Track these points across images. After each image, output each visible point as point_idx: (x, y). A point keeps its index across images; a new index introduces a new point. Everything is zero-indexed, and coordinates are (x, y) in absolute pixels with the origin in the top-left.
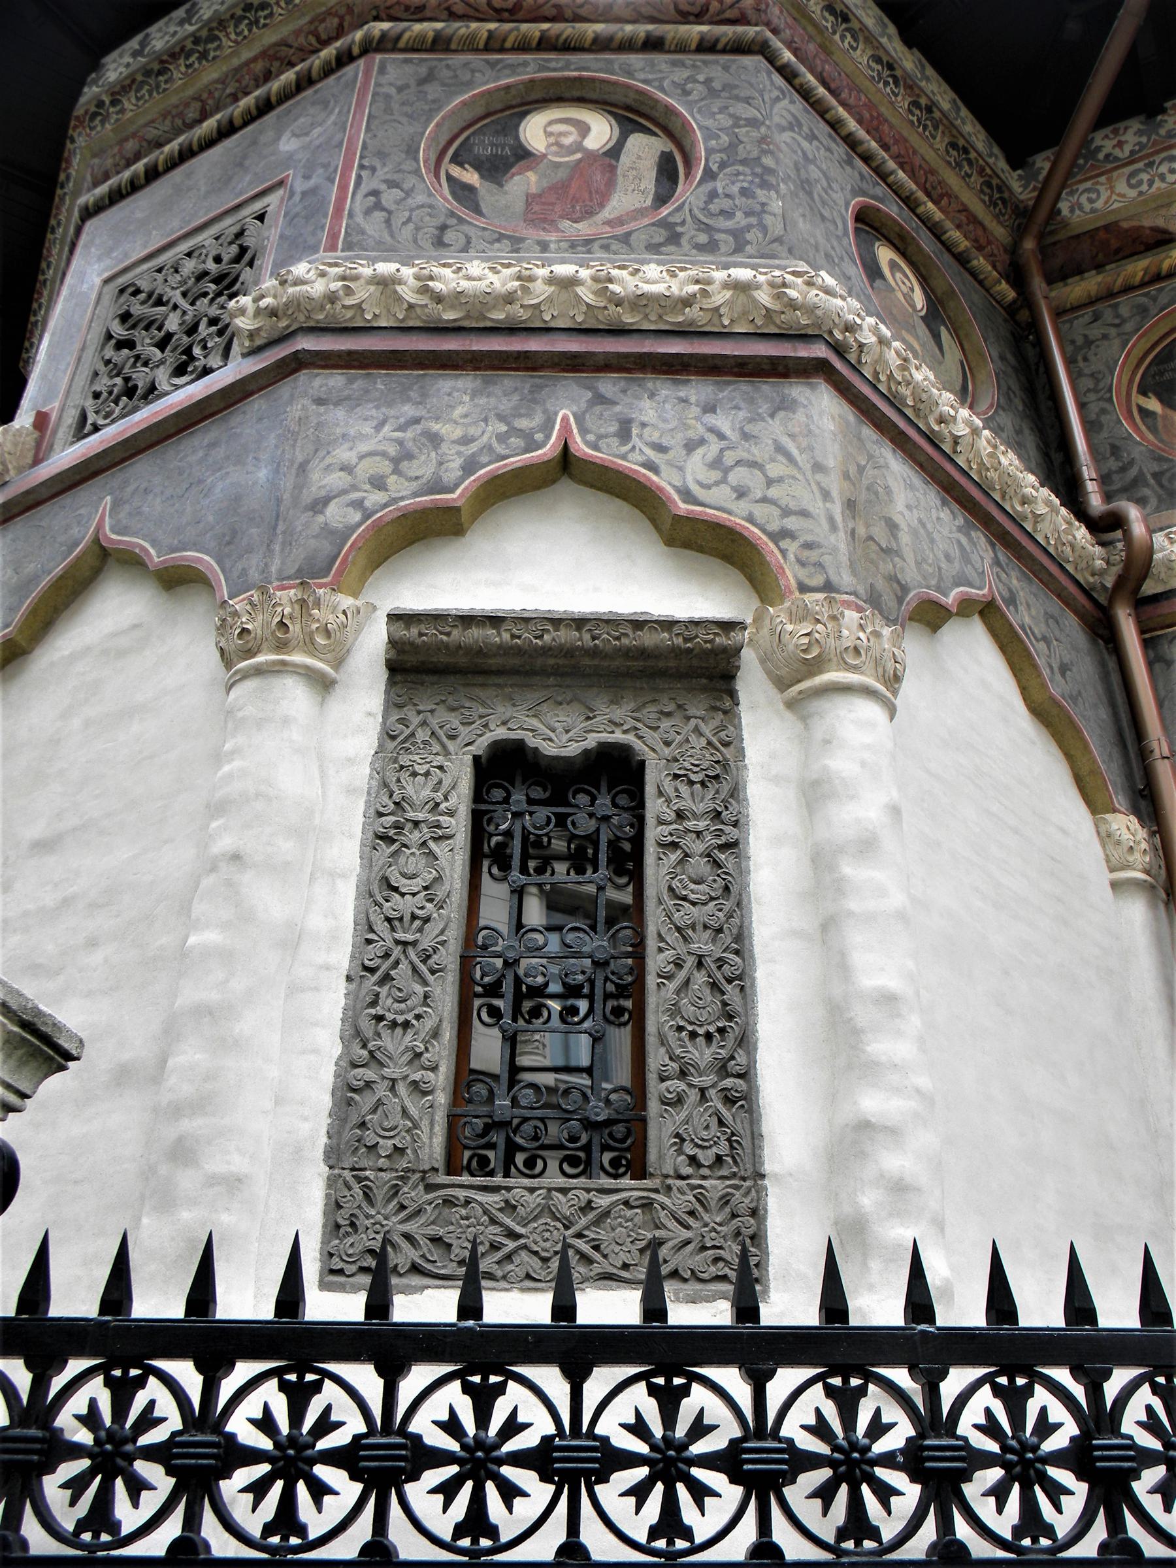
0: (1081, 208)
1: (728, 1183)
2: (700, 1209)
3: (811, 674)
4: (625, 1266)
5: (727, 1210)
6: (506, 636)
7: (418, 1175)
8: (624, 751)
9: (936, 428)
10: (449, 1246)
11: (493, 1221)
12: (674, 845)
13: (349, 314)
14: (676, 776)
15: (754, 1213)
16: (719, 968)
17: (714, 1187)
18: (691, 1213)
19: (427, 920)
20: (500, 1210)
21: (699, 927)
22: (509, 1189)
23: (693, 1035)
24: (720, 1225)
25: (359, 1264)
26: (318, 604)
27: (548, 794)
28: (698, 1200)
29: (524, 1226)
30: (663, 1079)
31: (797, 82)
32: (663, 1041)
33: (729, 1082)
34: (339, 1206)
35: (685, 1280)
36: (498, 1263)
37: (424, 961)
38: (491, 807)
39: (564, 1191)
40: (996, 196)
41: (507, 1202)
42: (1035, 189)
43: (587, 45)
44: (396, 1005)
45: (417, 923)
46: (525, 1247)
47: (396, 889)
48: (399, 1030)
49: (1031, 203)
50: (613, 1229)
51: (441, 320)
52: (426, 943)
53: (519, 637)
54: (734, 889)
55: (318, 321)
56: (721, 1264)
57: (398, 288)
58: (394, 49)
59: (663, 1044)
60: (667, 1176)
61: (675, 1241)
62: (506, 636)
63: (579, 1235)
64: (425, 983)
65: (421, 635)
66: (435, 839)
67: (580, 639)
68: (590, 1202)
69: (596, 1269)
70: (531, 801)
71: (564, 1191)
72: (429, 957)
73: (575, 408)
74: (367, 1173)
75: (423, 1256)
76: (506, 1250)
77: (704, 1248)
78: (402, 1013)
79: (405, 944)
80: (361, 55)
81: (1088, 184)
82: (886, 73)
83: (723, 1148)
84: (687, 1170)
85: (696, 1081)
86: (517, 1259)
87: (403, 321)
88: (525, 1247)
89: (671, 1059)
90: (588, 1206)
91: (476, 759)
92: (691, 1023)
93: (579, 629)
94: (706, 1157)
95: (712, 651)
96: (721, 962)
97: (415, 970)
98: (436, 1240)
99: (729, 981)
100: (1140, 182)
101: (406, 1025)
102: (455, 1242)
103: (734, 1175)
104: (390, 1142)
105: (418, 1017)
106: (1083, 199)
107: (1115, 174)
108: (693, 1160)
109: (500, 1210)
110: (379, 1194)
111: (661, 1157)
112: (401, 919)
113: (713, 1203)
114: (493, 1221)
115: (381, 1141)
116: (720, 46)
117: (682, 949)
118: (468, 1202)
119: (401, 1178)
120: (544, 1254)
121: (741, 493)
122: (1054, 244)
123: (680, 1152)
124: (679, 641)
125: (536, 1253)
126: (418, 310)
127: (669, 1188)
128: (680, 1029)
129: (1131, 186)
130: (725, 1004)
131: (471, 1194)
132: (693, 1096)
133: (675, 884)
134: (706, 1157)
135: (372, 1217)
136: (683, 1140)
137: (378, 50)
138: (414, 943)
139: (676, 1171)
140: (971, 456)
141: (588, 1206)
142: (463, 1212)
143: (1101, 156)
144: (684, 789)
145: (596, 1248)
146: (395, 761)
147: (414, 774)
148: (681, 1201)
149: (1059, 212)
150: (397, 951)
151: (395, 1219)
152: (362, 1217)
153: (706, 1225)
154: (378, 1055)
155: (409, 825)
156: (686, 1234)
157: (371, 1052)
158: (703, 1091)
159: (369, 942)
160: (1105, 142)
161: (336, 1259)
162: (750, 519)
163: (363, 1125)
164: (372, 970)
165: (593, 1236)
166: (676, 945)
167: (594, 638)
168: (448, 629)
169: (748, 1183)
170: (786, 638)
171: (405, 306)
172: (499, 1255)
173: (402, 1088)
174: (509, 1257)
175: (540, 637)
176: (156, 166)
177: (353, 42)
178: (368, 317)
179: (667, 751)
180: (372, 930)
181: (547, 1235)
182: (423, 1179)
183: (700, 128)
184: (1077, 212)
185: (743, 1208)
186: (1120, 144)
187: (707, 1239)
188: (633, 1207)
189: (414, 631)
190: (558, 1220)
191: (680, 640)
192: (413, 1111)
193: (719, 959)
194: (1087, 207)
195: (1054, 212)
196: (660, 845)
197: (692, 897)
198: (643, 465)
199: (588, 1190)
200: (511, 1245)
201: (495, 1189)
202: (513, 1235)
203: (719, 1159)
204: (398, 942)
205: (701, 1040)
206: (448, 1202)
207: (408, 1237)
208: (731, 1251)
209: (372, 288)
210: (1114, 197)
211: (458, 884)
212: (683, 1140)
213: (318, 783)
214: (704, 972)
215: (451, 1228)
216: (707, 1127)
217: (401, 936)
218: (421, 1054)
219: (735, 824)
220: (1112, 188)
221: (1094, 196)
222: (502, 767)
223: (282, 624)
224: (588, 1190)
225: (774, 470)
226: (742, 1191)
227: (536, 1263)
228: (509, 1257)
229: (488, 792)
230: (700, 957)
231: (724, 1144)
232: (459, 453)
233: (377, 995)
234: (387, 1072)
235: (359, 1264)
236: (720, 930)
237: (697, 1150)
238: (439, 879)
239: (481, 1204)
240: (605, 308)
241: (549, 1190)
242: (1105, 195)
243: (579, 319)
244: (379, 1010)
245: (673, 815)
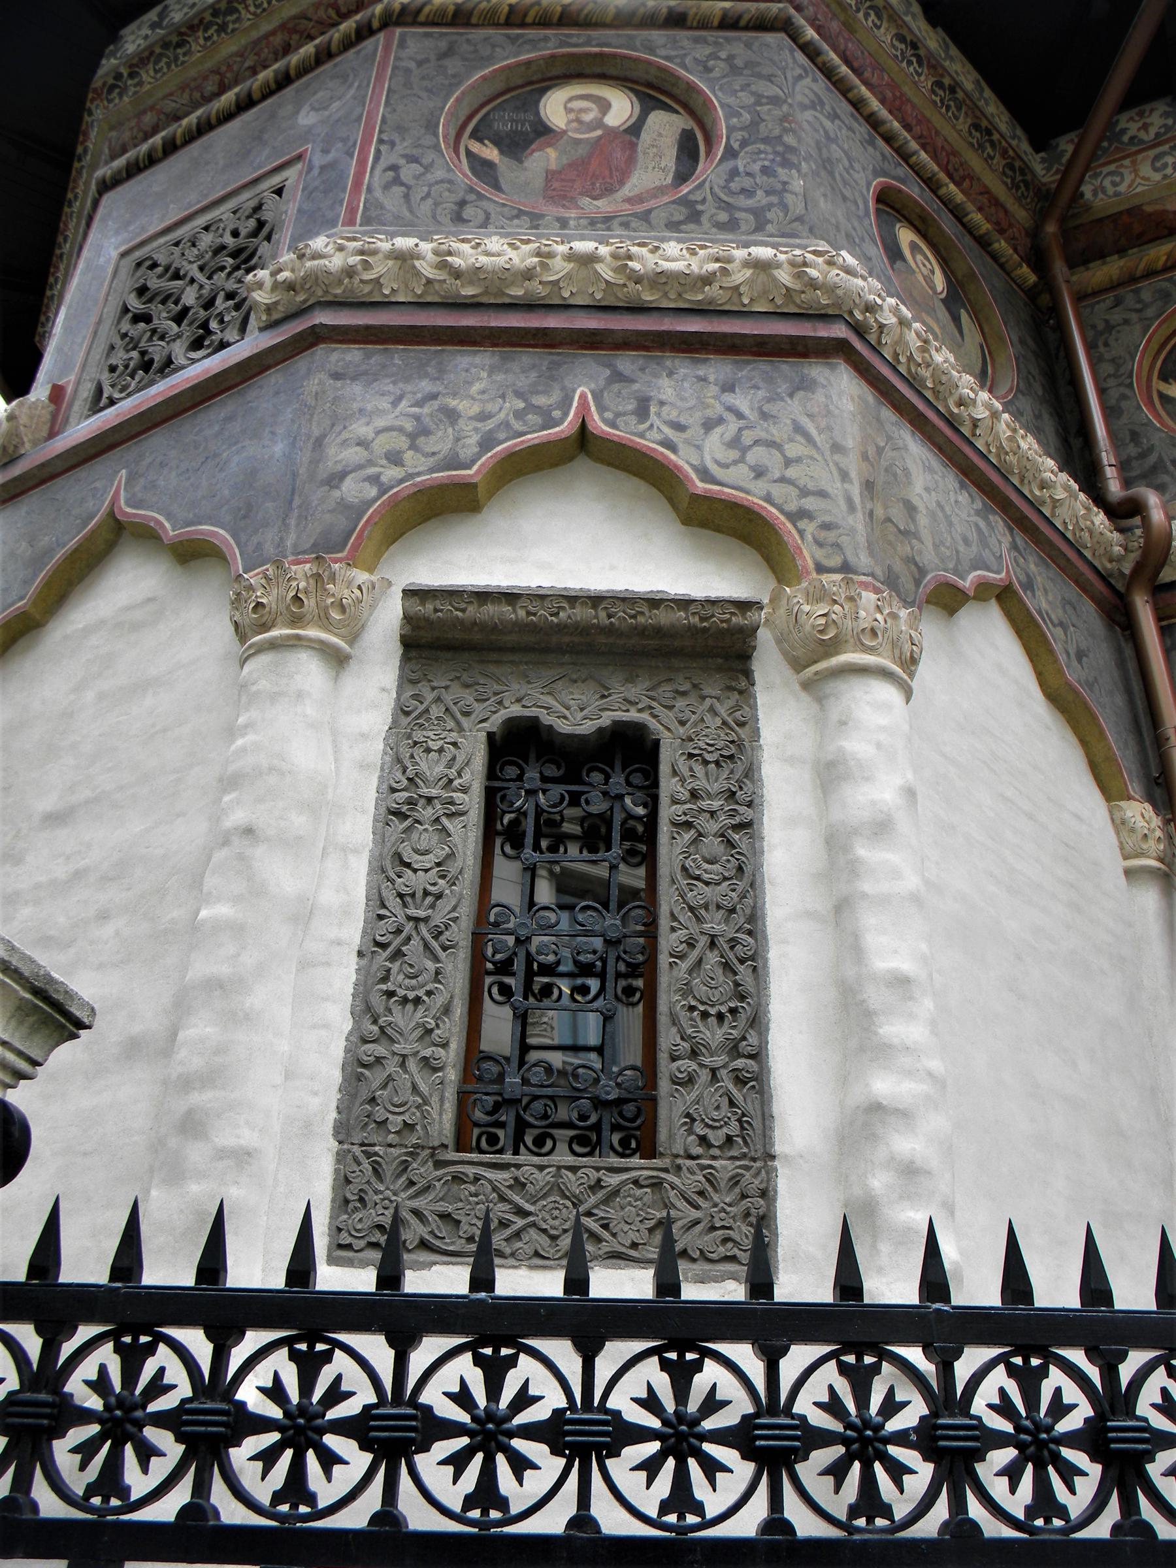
0: (1104, 191)
1: (738, 1163)
2: (710, 1189)
3: (828, 655)
4: (634, 1245)
5: (737, 1190)
6: (522, 613)
7: (428, 1151)
8: (639, 729)
9: (956, 410)
10: (458, 1222)
11: (503, 1198)
12: (688, 825)
13: (367, 289)
14: (691, 756)
15: (764, 1194)
16: (732, 948)
17: (724, 1167)
18: (701, 1193)
19: (439, 896)
20: (510, 1187)
21: (712, 907)
22: (518, 1166)
23: (705, 1015)
24: (730, 1205)
25: (368, 1239)
26: (333, 578)
27: (561, 772)
28: (708, 1180)
29: (534, 1204)
30: (674, 1059)
31: (819, 60)
32: (675, 1021)
33: (740, 1063)
34: (348, 1181)
35: (694, 1260)
36: (506, 1240)
37: (436, 938)
38: (505, 785)
39: (573, 1169)
40: (1019, 178)
41: (516, 1179)
42: (1058, 171)
43: (608, 20)
44: (407, 981)
45: (429, 899)
46: (534, 1225)
47: (408, 865)
48: (410, 1007)
49: (1054, 186)
50: (622, 1208)
51: (459, 296)
52: (438, 920)
53: (535, 614)
54: (748, 869)
55: (336, 296)
56: (730, 1245)
57: (417, 263)
58: (415, 23)
59: (674, 1024)
60: (677, 1156)
61: (685, 1221)
62: (522, 613)
63: (589, 1214)
64: (436, 959)
65: (436, 610)
66: (448, 816)
67: (596, 617)
68: (599, 1180)
69: (605, 1248)
70: (544, 779)
71: (573, 1169)
72: (441, 933)
73: (593, 386)
74: (377, 1148)
75: (432, 1232)
76: (515, 1228)
77: (713, 1228)
78: (413, 989)
79: (417, 920)
80: (380, 29)
81: (1112, 167)
82: (909, 52)
83: (733, 1128)
84: (697, 1150)
85: (707, 1061)
86: (525, 1237)
87: (420, 296)
88: (534, 1225)
89: (682, 1038)
90: (598, 1185)
91: (490, 736)
92: (703, 1003)
93: (595, 607)
94: (716, 1137)
95: (728, 630)
96: (733, 943)
97: (426, 946)
98: (445, 1217)
99: (742, 962)
100: (1165, 166)
101: (417, 1001)
102: (464, 1219)
103: (744, 1156)
104: (400, 1118)
105: (429, 993)
106: (1107, 183)
107: (1140, 157)
108: (703, 1140)
109: (510, 1187)
110: (389, 1170)
111: (671, 1136)
112: (413, 895)
113: (723, 1184)
114: (503, 1198)
115: (390, 1117)
116: (742, 23)
117: (694, 928)
118: (477, 1179)
119: (411, 1154)
120: (553, 1232)
121: (759, 473)
122: (1075, 228)
123: (690, 1131)
124: (695, 620)
125: (544, 1231)
126: (437, 286)
127: (679, 1168)
128: (692, 1008)
129: (1156, 170)
130: (737, 984)
132: (705, 1075)
133: (689, 863)
134: (716, 1137)
135: (381, 1192)
136: (693, 1120)
137: (398, 24)
138: (426, 920)
139: (686, 1151)
140: (990, 440)
141: (598, 1185)
142: (473, 1189)
143: (1125, 139)
144: (699, 769)
145: (605, 1227)
146: (409, 737)
147: (428, 750)
148: (692, 1181)
149: (1082, 195)
150: (409, 927)
151: (403, 1195)
152: (371, 1192)
153: (716, 1205)
154: (389, 1031)
155: (422, 801)
156: (695, 1214)
157: (381, 1028)
158: (714, 1071)
159: (381, 917)
160: (1129, 125)
161: (344, 1234)
162: (768, 499)
163: (373, 1100)
164: (383, 946)
166: (689, 925)
167: (610, 616)
168: (463, 605)
169: (759, 1164)
170: (803, 618)
171: (424, 281)
172: (508, 1232)
173: (412, 1065)
174: (517, 1235)
175: (556, 614)
176: (174, 139)
177: (373, 15)
178: (387, 292)
179: (681, 730)
180: (384, 906)
181: (556, 1213)
182: (432, 1155)
183: (722, 105)
184: (1101, 196)
185: (753, 1189)
186: (1145, 127)
187: (716, 1220)
188: (642, 1187)
189: (430, 607)
190: (567, 1198)
191: (697, 619)
192: (423, 1087)
193: (732, 939)
194: (1111, 190)
195: (1077, 195)
196: (674, 824)
197: (706, 876)
198: (661, 443)
199: (598, 1169)
200: (520, 1222)
202: (522, 1213)
203: (729, 1139)
204: (409, 918)
205: (712, 1021)
206: (457, 1179)
207: (416, 1213)
208: (740, 1232)
209: (390, 263)
210: (1138, 180)
211: (470, 861)
212: (693, 1120)
213: (332, 758)
214: (716, 952)
215: (460, 1205)
216: (718, 1108)
217: (412, 912)
218: (432, 1030)
219: (750, 805)
220: (1136, 171)
221: (1118, 179)
222: (516, 745)
223: (297, 599)
224: (598, 1169)
225: (792, 450)
226: (752, 1171)
227: (544, 1240)
228: (517, 1235)
229: (501, 770)
230: (713, 937)
231: (735, 1124)
232: (476, 429)
233: (388, 971)
234: (397, 1047)
235: (368, 1239)
236: (733, 911)
237: (707, 1131)
238: (451, 856)
239: (490, 1181)
240: (625, 285)
241: (559, 1168)
242: (1128, 178)
243: (598, 296)
244: (390, 986)
245: (687, 794)
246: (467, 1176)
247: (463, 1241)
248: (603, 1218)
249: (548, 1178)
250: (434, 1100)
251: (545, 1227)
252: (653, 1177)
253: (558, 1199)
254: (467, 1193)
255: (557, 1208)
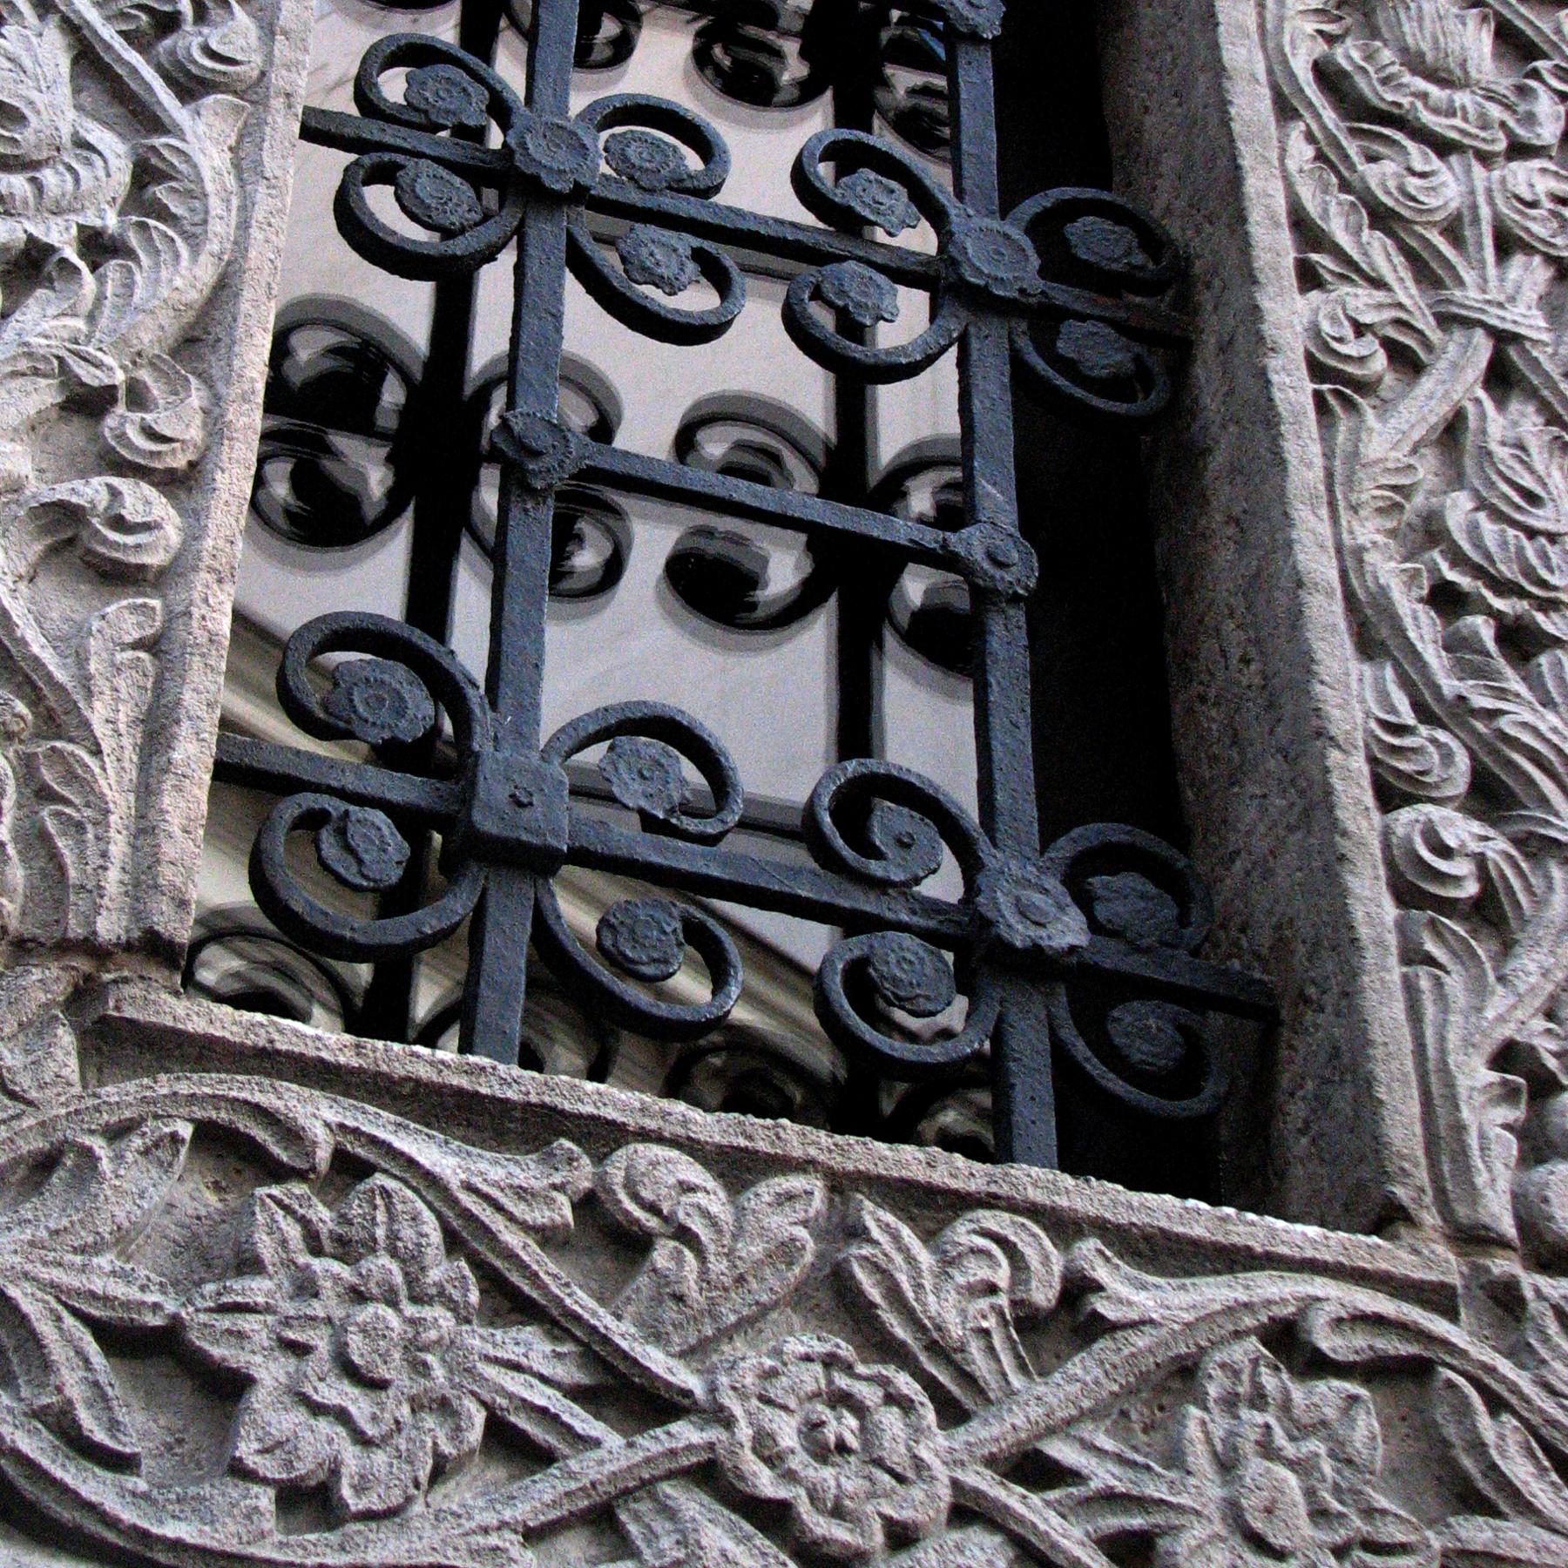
10: (226, 1389)
20: (547, 1237)
22: (603, 1136)
32: (1373, 634)
46: (709, 1475)
63: (1033, 1469)
68: (1078, 1288)
89: (1425, 714)
102: (270, 1372)
109: (547, 1237)
111: (1445, 1141)
114: (510, 1301)
118: (349, 1168)
127: (1506, 1302)
131: (380, 1123)
133: (1348, 54)
139: (1521, 1224)
141: (1071, 1321)
165: (1103, 1476)
166: (1390, 278)
172: (542, 1494)
181: (844, 1426)
182: (83, 995)
188: (1316, 1365)
190: (888, 1349)
197: (1427, 117)
201: (533, 1128)
230: (1503, 339)
239: (431, 1181)
246: (292, 1134)
247: (265, 1499)
248: (1110, 1499)
249: (784, 1224)
250: (111, 714)
251: (766, 1483)
252: (1377, 1321)
253: (846, 1351)
254: (293, 1231)
255: (842, 1400)
